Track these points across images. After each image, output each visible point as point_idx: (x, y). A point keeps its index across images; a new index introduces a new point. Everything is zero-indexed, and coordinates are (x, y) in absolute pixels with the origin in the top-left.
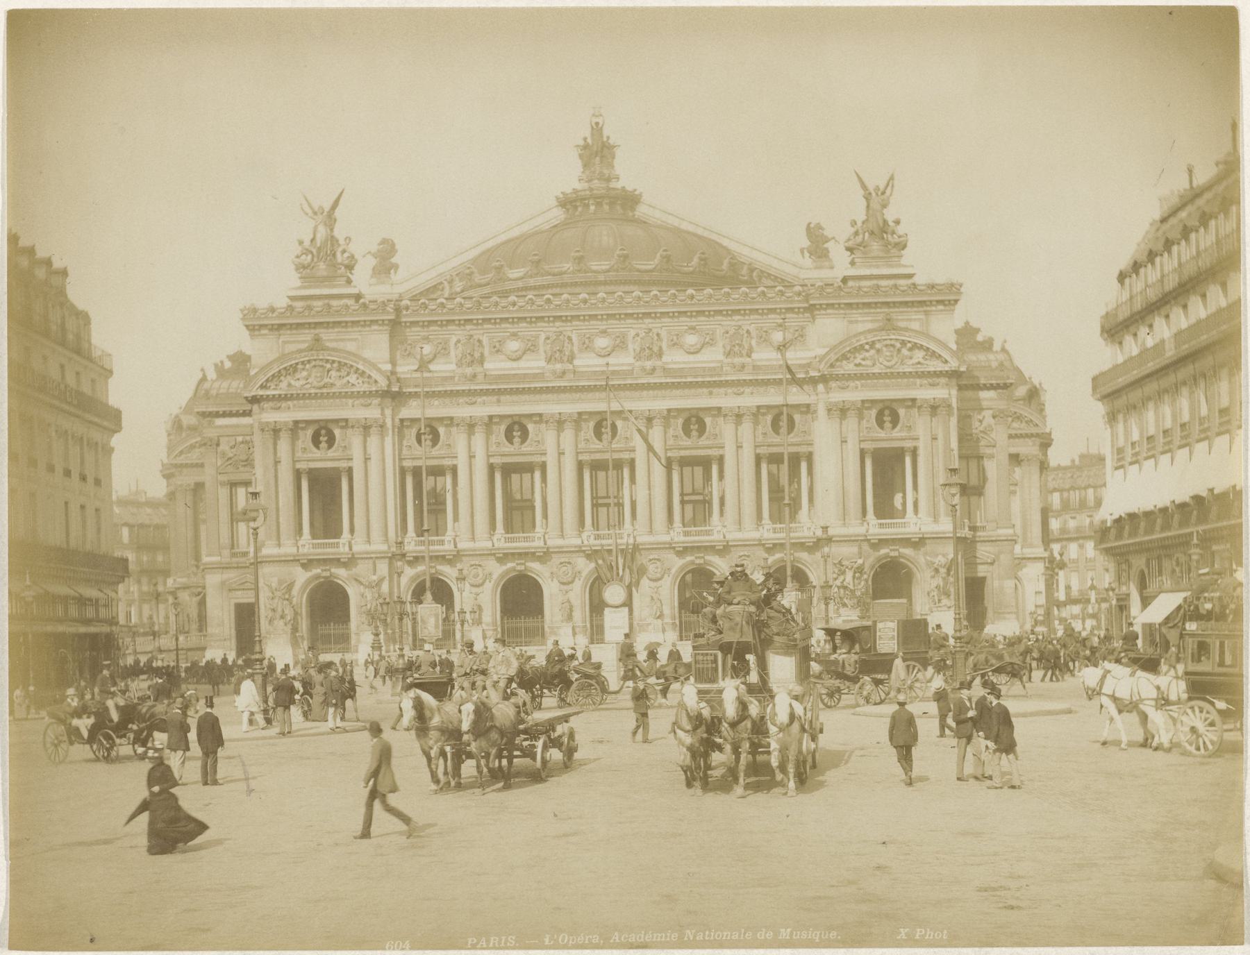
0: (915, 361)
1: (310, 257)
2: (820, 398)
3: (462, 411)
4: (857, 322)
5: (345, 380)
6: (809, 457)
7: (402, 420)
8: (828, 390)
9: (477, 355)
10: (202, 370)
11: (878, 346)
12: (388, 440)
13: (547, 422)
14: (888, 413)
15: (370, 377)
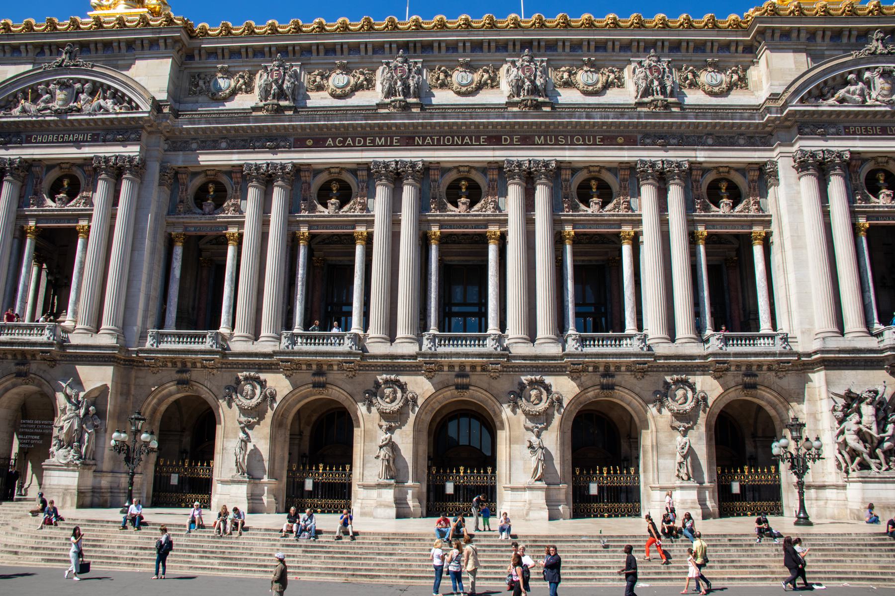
15: (131, 101)
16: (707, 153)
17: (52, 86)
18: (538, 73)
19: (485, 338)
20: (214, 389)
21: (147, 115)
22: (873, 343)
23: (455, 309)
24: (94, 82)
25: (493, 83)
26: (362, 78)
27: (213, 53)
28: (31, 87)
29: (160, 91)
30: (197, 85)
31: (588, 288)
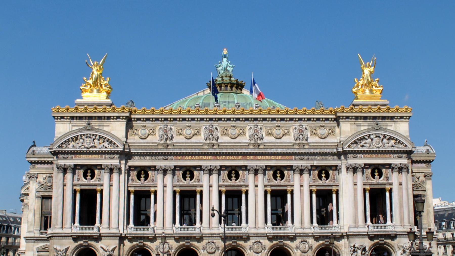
0: (390, 144)
1: (89, 86)
2: (343, 163)
3: (160, 163)
4: (361, 125)
5: (102, 145)
6: (337, 192)
7: (130, 167)
8: (346, 158)
9: (170, 135)
10: (34, 142)
11: (372, 137)
12: (122, 176)
13: (204, 170)
14: (377, 170)
15: (114, 144)
16: (318, 162)
17: (83, 137)
18: (259, 132)
19: (241, 228)
20: (152, 246)
21: (122, 150)
22: (366, 229)
23: (229, 212)
24: (99, 136)
25: (244, 134)
26: (196, 131)
27: (139, 119)
28: (75, 137)
29: (122, 137)
30: (134, 132)
31: (279, 199)
